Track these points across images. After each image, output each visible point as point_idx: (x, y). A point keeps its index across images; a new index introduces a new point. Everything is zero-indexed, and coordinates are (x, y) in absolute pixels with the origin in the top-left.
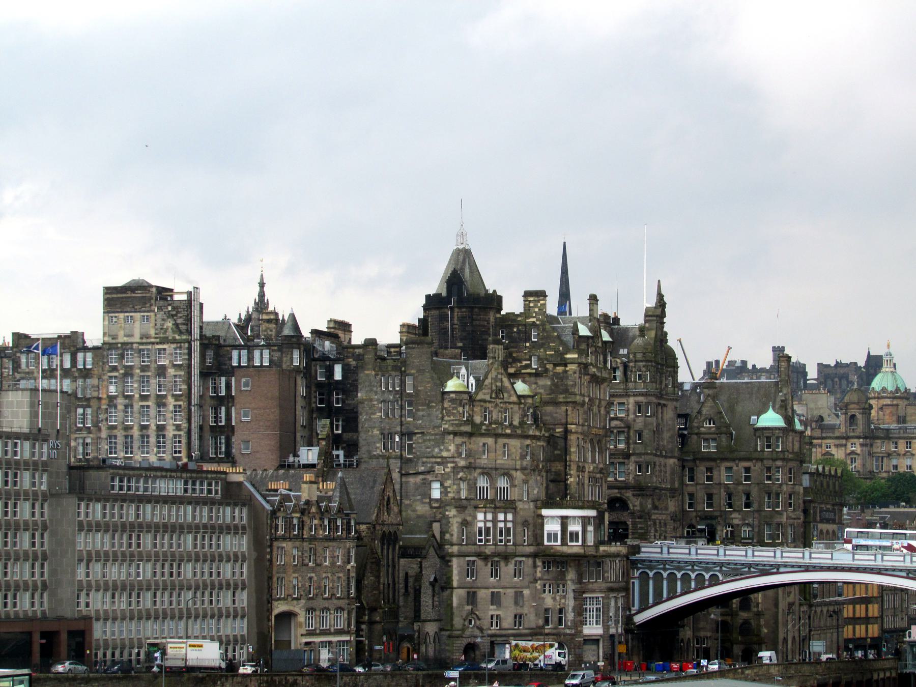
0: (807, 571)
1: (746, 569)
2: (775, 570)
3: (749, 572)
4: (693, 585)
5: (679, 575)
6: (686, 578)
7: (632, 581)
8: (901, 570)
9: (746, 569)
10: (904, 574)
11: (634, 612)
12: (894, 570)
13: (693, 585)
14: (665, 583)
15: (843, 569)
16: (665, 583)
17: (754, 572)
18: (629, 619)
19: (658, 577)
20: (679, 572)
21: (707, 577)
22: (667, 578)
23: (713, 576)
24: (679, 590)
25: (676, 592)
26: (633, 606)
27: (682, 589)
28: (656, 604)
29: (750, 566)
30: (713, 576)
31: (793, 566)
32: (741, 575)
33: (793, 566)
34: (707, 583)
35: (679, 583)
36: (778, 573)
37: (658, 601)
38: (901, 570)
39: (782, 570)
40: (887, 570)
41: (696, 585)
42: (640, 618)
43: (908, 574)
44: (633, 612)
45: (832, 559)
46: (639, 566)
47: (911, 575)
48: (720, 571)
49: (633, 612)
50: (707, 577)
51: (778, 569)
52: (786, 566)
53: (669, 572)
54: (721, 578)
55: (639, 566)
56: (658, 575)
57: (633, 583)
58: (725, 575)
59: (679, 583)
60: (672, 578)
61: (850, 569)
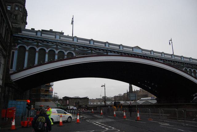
0: (121, 55)
1: (90, 51)
2: (106, 54)
3: (92, 53)
4: (56, 57)
5: (47, 51)
6: (52, 53)
7: (12, 51)
8: (161, 59)
9: (90, 51)
10: (162, 62)
11: (12, 72)
12: (158, 59)
13: (56, 57)
14: (37, 55)
16: (37, 55)
17: (94, 54)
18: (7, 76)
19: (32, 51)
21: (66, 53)
23: (70, 54)
24: (46, 60)
25: (44, 61)
26: (12, 68)
27: (48, 60)
28: (29, 67)
31: (114, 52)
32: (86, 54)
34: (66, 57)
35: (47, 56)
36: (107, 55)
37: (31, 65)
39: (109, 54)
42: (16, 77)
43: (164, 62)
44: (11, 72)
45: (133, 51)
46: (19, 41)
48: (74, 51)
49: (11, 72)
50: (66, 53)
51: (107, 53)
52: (111, 51)
54: (74, 55)
55: (19, 41)
57: (13, 52)
58: (77, 53)
59: (47, 56)
60: (43, 52)
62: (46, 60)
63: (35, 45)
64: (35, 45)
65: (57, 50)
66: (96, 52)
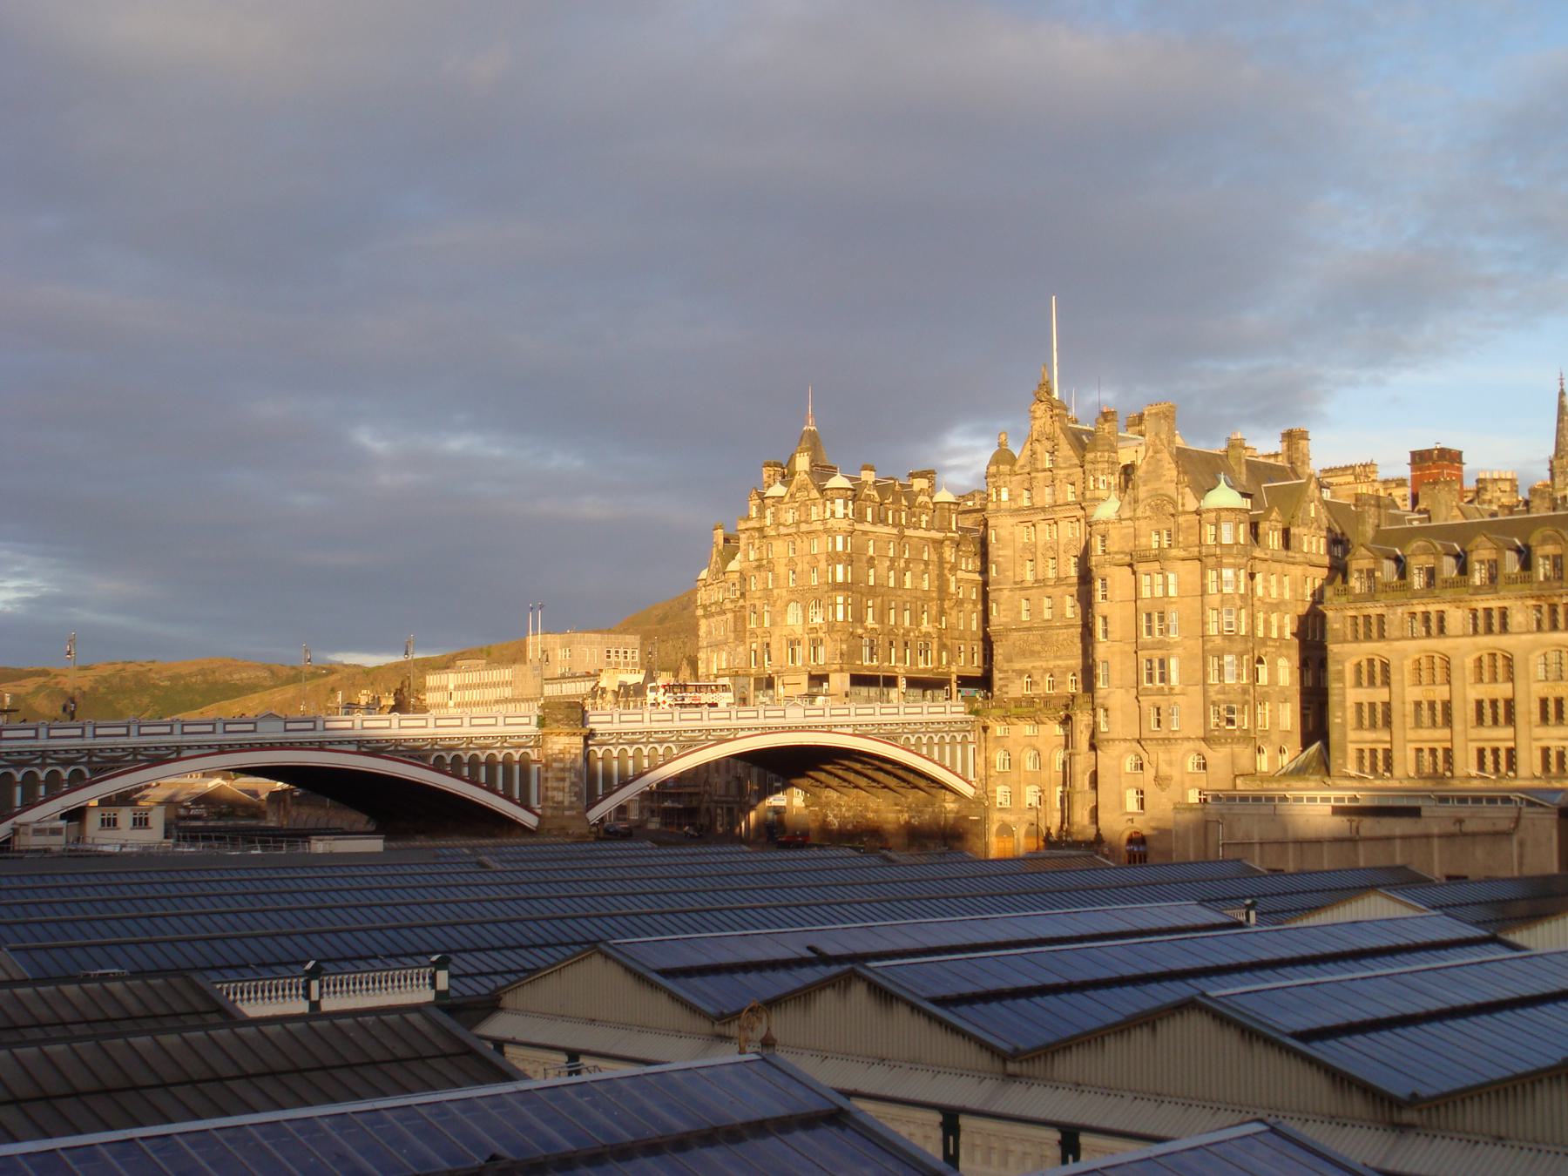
4: (42, 790)
6: (30, 781)
10: (353, 748)
12: (340, 743)
13: (42, 790)
15: (272, 747)
20: (18, 771)
21: (65, 774)
22: (22, 783)
29: (135, 751)
30: (54, 778)
31: (199, 747)
33: (199, 747)
38: (350, 742)
39: (186, 753)
40: (330, 743)
41: (47, 792)
43: (359, 747)
47: (363, 749)
50: (65, 774)
51: (179, 753)
52: (189, 747)
53: (49, 769)
54: (88, 775)
56: (31, 776)
61: (282, 746)
62: (18, 802)
63: (36, 765)
64: (36, 765)
65: (42, 770)
66: (146, 755)
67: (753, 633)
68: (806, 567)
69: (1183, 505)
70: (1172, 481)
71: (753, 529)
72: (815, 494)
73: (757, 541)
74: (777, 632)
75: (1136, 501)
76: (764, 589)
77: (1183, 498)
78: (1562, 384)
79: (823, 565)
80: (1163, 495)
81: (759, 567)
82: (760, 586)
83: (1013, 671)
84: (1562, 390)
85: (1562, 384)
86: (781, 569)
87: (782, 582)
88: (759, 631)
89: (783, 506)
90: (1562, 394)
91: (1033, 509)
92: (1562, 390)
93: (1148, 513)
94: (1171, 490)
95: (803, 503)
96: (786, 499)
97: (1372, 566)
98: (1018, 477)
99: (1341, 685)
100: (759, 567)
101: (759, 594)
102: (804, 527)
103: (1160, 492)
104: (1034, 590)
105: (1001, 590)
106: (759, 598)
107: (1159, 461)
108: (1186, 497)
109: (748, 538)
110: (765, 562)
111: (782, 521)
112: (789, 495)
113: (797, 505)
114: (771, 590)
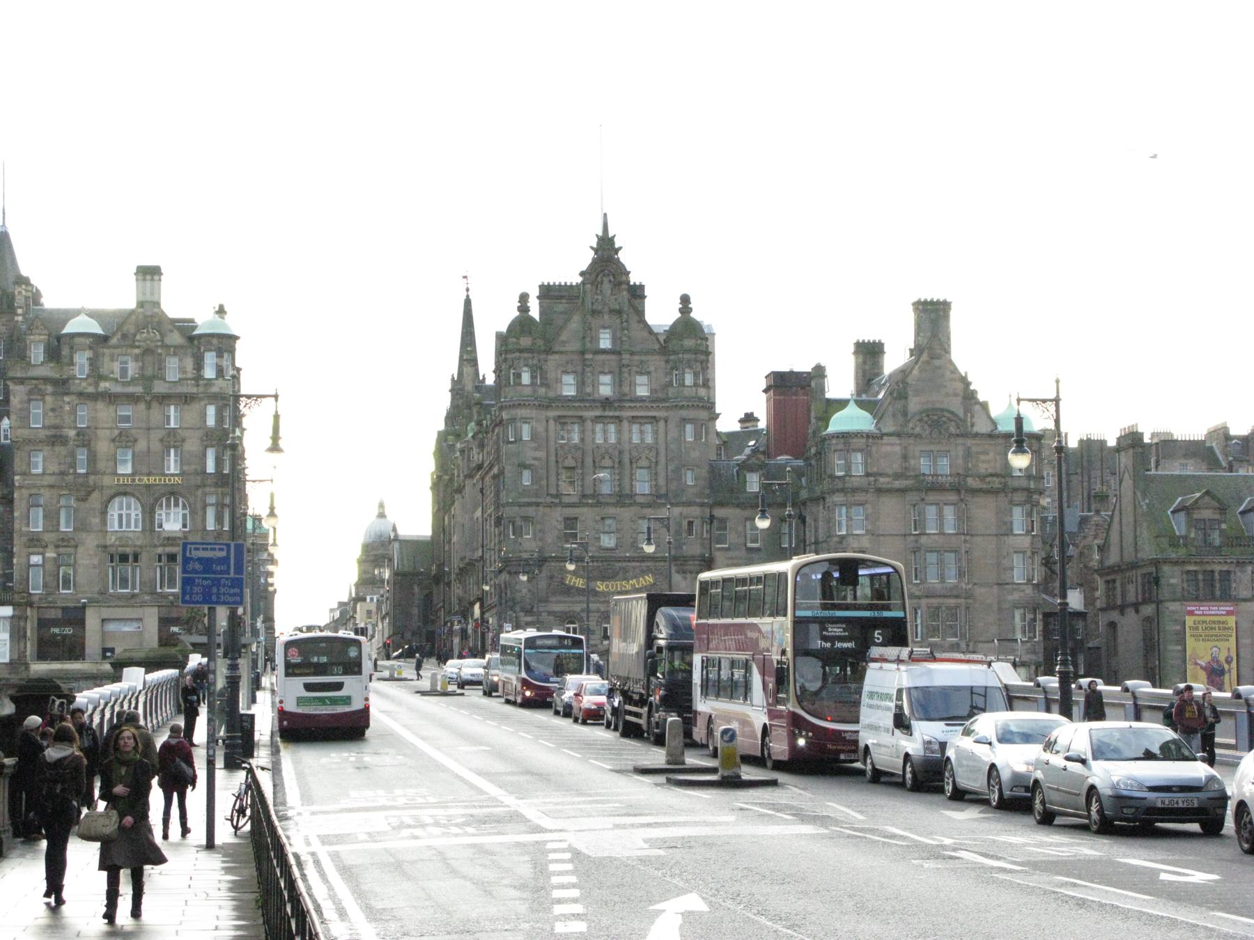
67: (35, 542)
68: (156, 446)
69: (972, 425)
70: (956, 395)
71: (46, 380)
72: (176, 338)
73: (49, 399)
74: (90, 542)
75: (905, 414)
76: (62, 473)
77: (972, 417)
78: (468, 290)
79: (192, 445)
80: (943, 410)
81: (56, 439)
82: (54, 468)
83: (550, 613)
84: (468, 296)
85: (468, 290)
86: (103, 447)
87: (101, 465)
88: (48, 537)
89: (106, 351)
90: (468, 303)
91: (582, 401)
92: (468, 296)
93: (918, 430)
94: (956, 405)
95: (148, 351)
96: (114, 341)
97: (1217, 516)
98: (557, 356)
99: (1179, 648)
100: (56, 439)
101: (49, 480)
102: (159, 388)
103: (938, 406)
104: (585, 510)
105: (538, 504)
106: (52, 487)
107: (939, 368)
108: (976, 416)
109: (30, 392)
110: (72, 433)
111: (104, 370)
112: (119, 336)
113: (137, 351)
114: (87, 475)
